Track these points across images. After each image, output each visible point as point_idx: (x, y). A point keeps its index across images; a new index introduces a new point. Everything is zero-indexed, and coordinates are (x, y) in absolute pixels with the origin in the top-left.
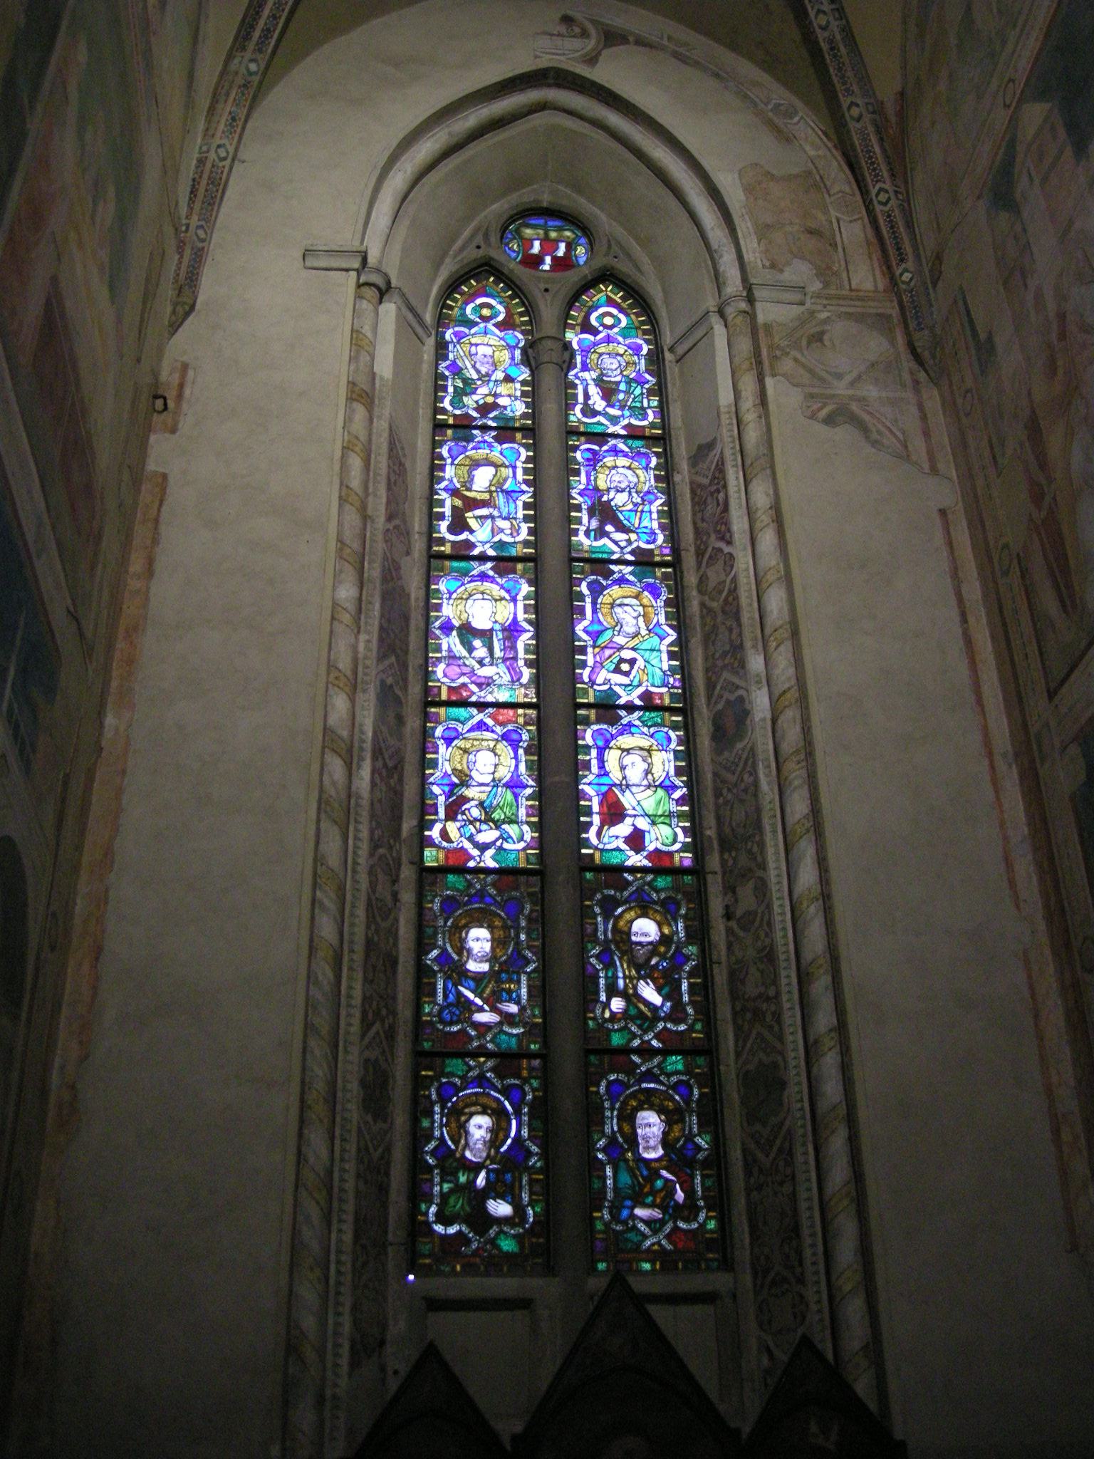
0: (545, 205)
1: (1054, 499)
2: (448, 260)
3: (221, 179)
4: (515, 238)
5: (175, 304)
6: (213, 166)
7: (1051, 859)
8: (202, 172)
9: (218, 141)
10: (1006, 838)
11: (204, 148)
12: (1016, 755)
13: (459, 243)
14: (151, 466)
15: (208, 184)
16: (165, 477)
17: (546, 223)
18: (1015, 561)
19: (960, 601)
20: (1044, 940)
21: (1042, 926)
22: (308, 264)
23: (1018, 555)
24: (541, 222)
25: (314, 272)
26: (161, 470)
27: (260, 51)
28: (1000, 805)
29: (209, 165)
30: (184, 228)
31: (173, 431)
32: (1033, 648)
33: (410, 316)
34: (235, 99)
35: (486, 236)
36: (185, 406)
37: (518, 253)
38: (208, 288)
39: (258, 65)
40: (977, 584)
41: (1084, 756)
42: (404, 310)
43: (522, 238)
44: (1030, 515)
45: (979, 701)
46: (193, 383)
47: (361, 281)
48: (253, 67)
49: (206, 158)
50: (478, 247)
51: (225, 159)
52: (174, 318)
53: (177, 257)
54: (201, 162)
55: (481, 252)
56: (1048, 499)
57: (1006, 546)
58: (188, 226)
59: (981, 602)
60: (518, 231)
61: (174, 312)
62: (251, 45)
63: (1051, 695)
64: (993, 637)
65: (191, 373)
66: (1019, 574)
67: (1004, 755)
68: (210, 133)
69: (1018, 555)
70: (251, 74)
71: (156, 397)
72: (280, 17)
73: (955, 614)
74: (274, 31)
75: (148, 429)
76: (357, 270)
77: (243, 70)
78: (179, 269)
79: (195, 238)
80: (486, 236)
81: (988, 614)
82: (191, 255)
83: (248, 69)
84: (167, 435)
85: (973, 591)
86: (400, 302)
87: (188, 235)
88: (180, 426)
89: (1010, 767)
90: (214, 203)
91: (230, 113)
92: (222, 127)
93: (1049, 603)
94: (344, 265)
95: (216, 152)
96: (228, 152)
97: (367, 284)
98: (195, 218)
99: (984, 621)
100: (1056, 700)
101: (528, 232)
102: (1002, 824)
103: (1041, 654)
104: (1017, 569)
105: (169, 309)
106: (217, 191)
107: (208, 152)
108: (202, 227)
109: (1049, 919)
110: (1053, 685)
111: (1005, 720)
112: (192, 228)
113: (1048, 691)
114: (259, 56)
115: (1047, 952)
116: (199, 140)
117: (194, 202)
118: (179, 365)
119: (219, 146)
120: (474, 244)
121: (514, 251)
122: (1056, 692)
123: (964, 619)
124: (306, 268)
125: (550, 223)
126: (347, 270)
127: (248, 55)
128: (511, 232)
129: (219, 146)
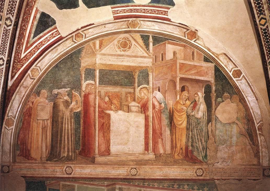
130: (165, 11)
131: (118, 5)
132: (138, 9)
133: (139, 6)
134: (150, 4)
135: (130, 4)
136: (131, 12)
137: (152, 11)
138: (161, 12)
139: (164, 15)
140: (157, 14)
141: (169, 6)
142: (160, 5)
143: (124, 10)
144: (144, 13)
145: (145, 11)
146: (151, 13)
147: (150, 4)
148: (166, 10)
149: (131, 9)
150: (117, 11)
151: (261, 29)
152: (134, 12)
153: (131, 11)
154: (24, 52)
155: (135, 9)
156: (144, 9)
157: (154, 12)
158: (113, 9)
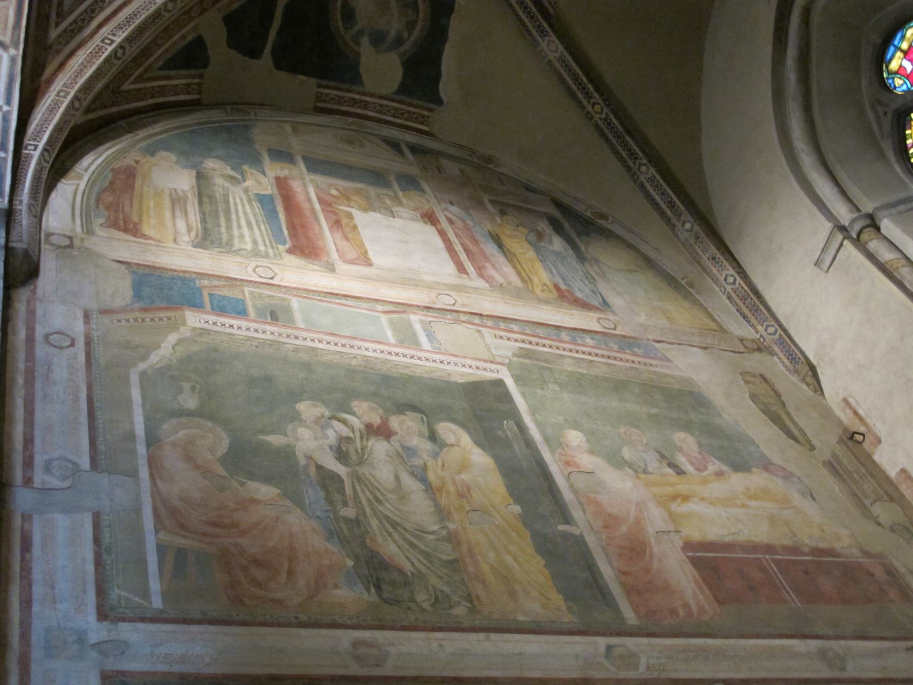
0: (880, 41)
2: (882, 144)
3: (745, 291)
4: (893, 78)
5: (803, 380)
6: (735, 292)
8: (735, 302)
9: (722, 279)
11: (723, 290)
13: (875, 126)
14: (892, 473)
15: (744, 303)
16: (903, 471)
17: (895, 46)
22: (825, 268)
24: (892, 49)
25: (831, 268)
26: (898, 469)
27: (680, 215)
29: (733, 295)
30: (762, 340)
31: (879, 441)
33: (902, 208)
34: (702, 250)
35: (880, 103)
36: (868, 421)
37: (905, 82)
38: (809, 346)
39: (689, 222)
42: (894, 211)
43: (896, 73)
46: (858, 404)
47: (855, 236)
48: (688, 226)
49: (728, 293)
50: (885, 113)
51: (735, 280)
52: (811, 387)
53: (775, 358)
54: (729, 298)
55: (889, 115)
58: (761, 336)
60: (889, 73)
61: (808, 384)
62: (674, 220)
65: (851, 400)
68: (715, 278)
70: (691, 230)
71: (851, 438)
72: (665, 190)
74: (672, 198)
75: (869, 456)
76: (844, 238)
77: (687, 234)
78: (783, 362)
79: (771, 337)
80: (880, 103)
82: (779, 347)
83: (687, 231)
84: (880, 447)
86: (886, 213)
87: (767, 340)
88: (879, 434)
90: (758, 306)
91: (709, 259)
92: (714, 270)
94: (837, 246)
95: (728, 284)
96: (732, 276)
97: (859, 235)
98: (759, 327)
101: (894, 65)
105: (805, 387)
106: (751, 299)
107: (725, 290)
108: (768, 326)
112: (764, 334)
114: (683, 218)
116: (717, 289)
117: (750, 321)
118: (843, 404)
119: (725, 280)
120: (881, 114)
121: (902, 85)
124: (827, 272)
125: (896, 42)
126: (841, 245)
127: (679, 225)
128: (888, 78)
129: (725, 280)
130: (423, 116)
131: (333, 84)
132: (368, 102)
133: (372, 96)
134: (396, 97)
135: (355, 88)
136: (353, 106)
137: (396, 113)
138: (415, 116)
139: (422, 123)
140: (407, 119)
141: (432, 106)
142: (415, 102)
143: (340, 97)
144: (380, 112)
145: (382, 109)
146: (394, 117)
147: (396, 97)
148: (425, 113)
149: (354, 100)
150: (326, 95)
151: (600, 119)
152: (359, 107)
153: (355, 102)
154: (132, 83)
155: (362, 101)
156: (381, 106)
157: (402, 114)
158: (320, 90)
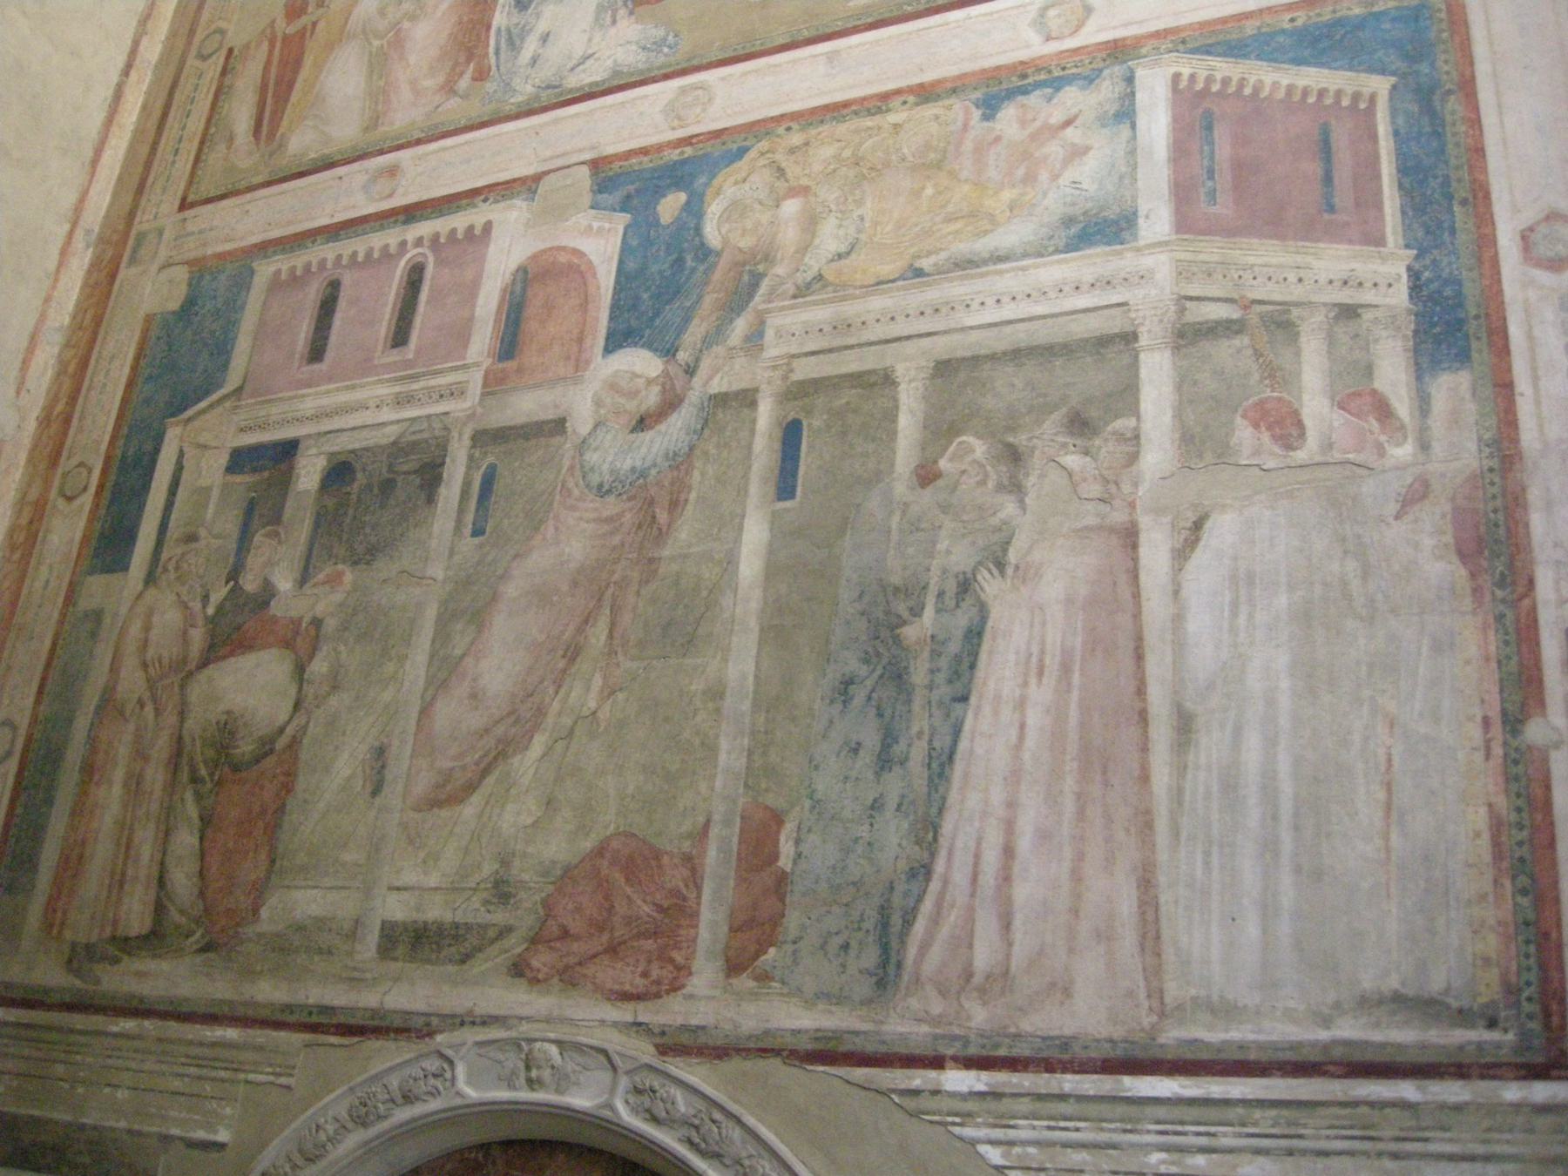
1: (314, 24)
7: (84, 364)
10: (42, 317)
12: (102, 240)
18: (224, 52)
19: (133, 52)
20: (27, 441)
21: (31, 425)
23: (231, 51)
28: (56, 280)
32: (189, 149)
40: (160, 46)
41: (190, 285)
44: (273, 22)
45: (95, 162)
56: (305, 20)
57: (222, 32)
59: (152, 67)
63: (184, 205)
64: (144, 107)
66: (219, 69)
67: (88, 232)
69: (231, 51)
73: (121, 61)
81: (152, 84)
85: (152, 51)
89: (88, 246)
93: (241, 114)
99: (144, 88)
100: (188, 213)
102: (48, 300)
103: (197, 160)
104: (222, 60)
109: (45, 421)
110: (191, 198)
111: (108, 198)
113: (184, 199)
115: (23, 457)
122: (192, 205)
123: (126, 71)
